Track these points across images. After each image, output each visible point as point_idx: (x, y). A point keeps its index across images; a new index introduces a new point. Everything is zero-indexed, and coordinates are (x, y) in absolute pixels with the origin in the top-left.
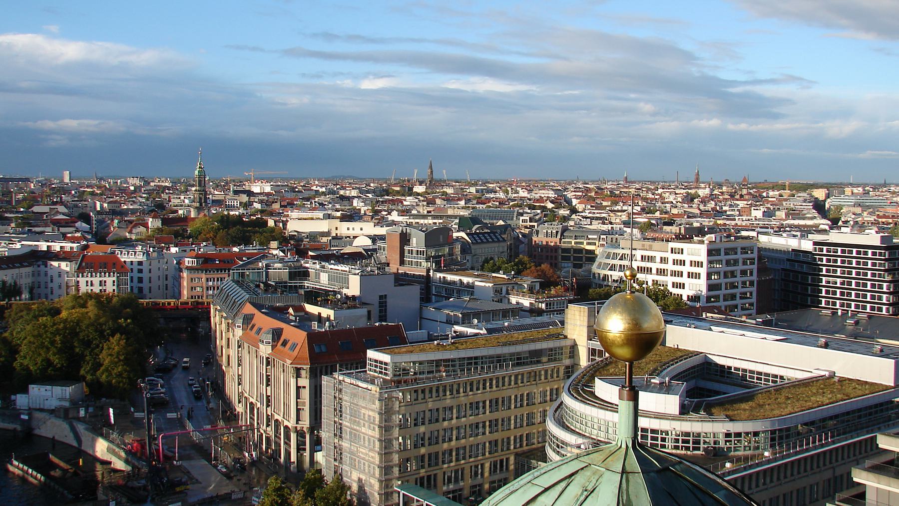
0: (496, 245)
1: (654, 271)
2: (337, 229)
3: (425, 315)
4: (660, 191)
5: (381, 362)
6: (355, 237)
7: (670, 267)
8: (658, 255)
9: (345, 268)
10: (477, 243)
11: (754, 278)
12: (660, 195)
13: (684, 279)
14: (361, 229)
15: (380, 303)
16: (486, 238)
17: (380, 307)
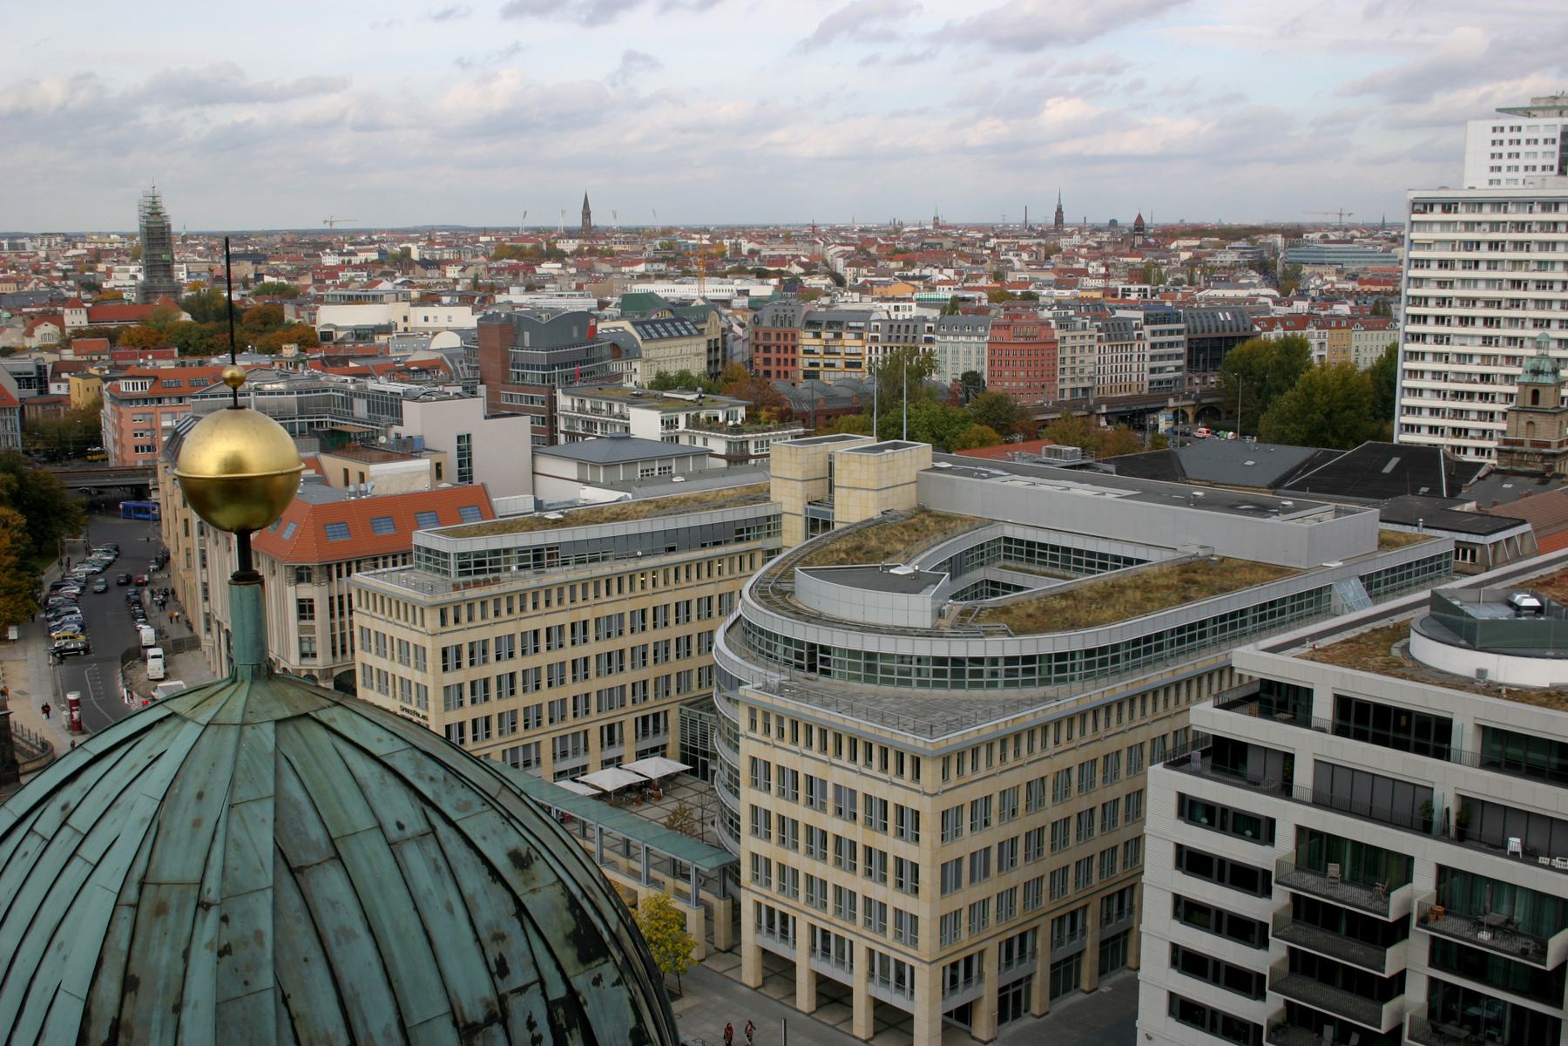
0: (687, 341)
2: (405, 319)
3: (539, 470)
4: (993, 242)
5: (437, 553)
6: (435, 334)
9: (398, 387)
10: (652, 338)
12: (993, 249)
16: (657, 331)
17: (459, 456)
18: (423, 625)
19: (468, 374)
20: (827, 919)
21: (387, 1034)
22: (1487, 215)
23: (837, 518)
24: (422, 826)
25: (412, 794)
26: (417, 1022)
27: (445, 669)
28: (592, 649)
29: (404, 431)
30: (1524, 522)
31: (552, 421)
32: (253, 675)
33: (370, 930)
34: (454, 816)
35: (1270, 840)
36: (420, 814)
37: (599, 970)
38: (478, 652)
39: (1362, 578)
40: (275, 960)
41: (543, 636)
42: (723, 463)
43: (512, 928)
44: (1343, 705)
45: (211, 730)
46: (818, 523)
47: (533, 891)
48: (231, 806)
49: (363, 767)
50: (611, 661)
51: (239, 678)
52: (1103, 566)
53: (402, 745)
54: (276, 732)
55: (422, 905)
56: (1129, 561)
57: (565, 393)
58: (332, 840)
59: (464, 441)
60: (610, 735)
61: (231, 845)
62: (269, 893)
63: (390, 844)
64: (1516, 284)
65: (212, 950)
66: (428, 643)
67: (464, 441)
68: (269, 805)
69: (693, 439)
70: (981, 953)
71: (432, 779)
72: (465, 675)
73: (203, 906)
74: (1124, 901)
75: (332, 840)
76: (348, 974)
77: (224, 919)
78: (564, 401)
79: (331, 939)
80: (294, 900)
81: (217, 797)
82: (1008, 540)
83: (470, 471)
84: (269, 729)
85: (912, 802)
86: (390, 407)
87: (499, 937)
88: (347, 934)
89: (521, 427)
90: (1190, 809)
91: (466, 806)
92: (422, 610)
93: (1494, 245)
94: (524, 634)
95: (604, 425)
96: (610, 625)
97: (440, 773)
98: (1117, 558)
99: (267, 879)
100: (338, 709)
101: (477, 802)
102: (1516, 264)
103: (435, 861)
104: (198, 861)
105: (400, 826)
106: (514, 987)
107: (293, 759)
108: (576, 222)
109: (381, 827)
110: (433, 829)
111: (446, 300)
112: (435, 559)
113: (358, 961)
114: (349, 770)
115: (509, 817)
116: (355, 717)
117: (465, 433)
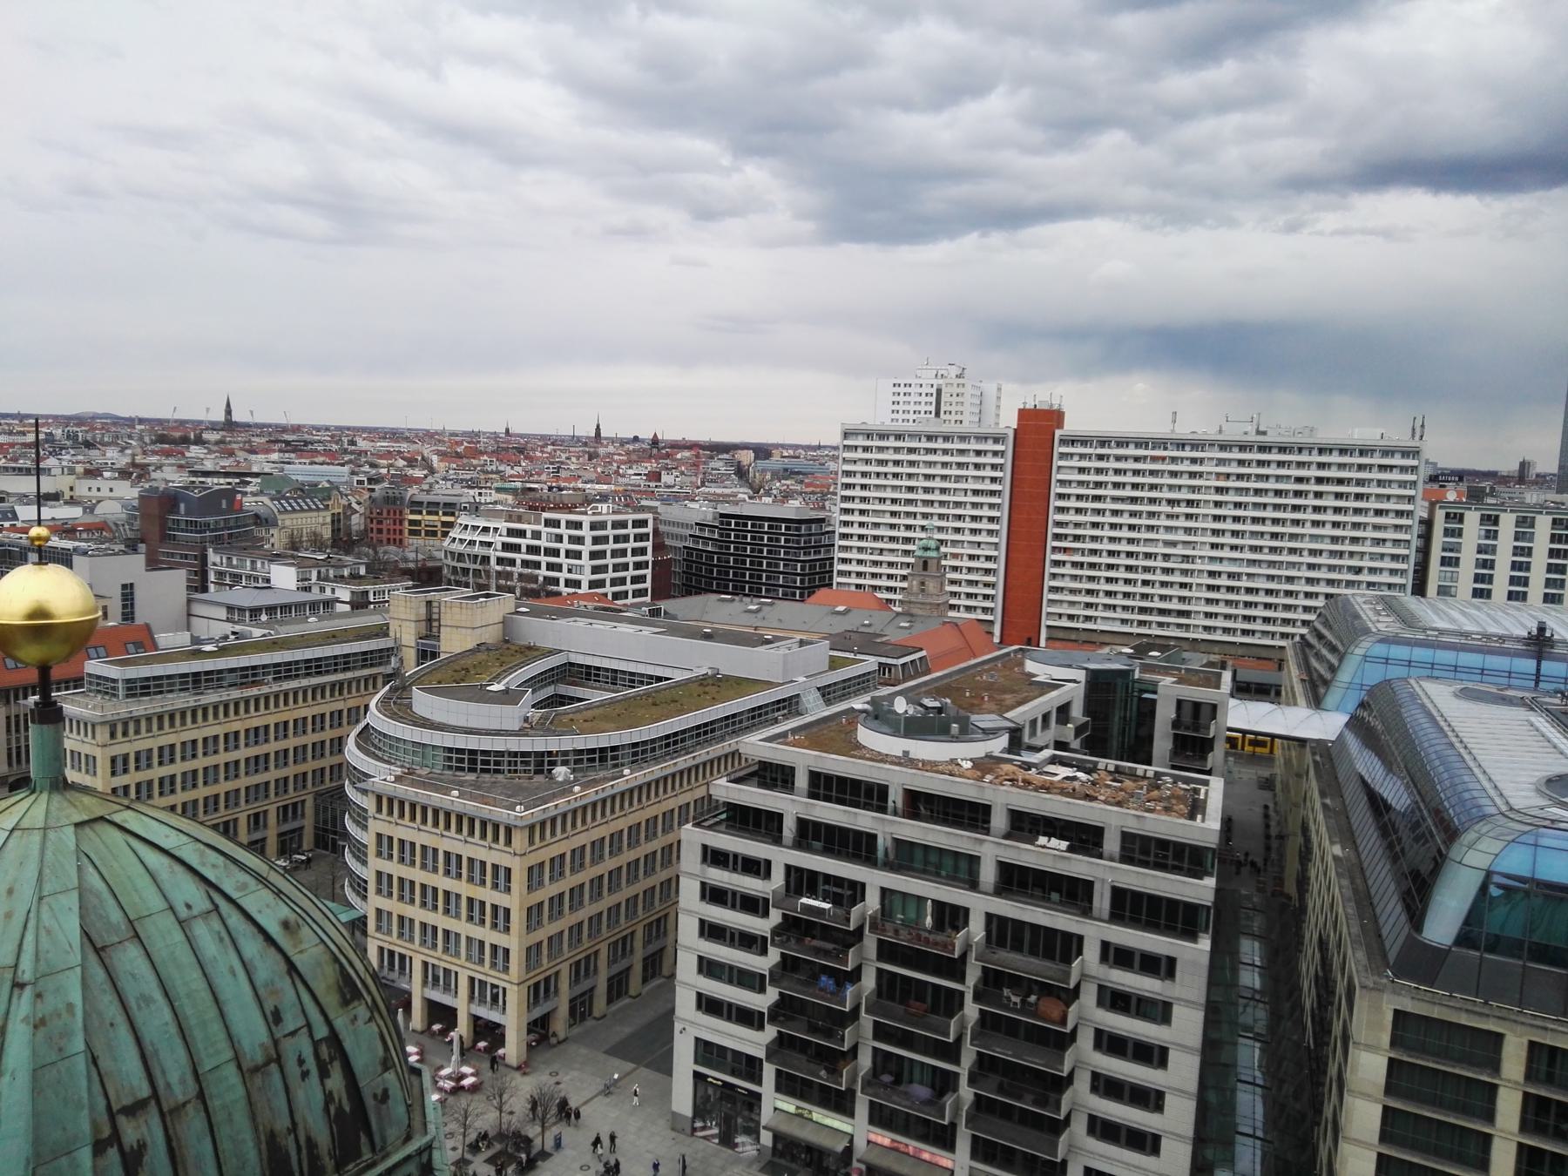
0: (315, 514)
1: (524, 549)
2: (71, 489)
5: (106, 679)
6: (99, 502)
7: (543, 543)
8: (528, 527)
11: (649, 557)
13: (562, 559)
14: (111, 490)
15: (123, 595)
17: (123, 600)
18: (94, 737)
19: (130, 535)
20: (439, 958)
21: (183, 1082)
22: (892, 443)
23: (442, 649)
24: (208, 905)
25: (197, 879)
26: (208, 1068)
27: (113, 774)
28: (242, 753)
30: (921, 649)
31: (204, 574)
32: (51, 786)
33: (166, 994)
34: (235, 895)
35: (768, 875)
36: (204, 896)
37: (354, 1012)
38: (143, 759)
39: (819, 689)
40: (85, 1026)
41: (200, 745)
42: (347, 608)
43: (285, 984)
44: (815, 777)
45: (17, 833)
46: (424, 655)
47: (301, 952)
48: (41, 898)
49: (152, 858)
50: (258, 763)
51: (38, 789)
52: (642, 683)
53: (185, 839)
54: (76, 834)
55: (209, 970)
56: (659, 679)
57: (216, 551)
58: (130, 922)
59: (128, 592)
60: (257, 820)
61: (43, 933)
62: (78, 970)
63: (180, 922)
64: (910, 489)
65: (28, 1024)
66: (98, 753)
67: (128, 592)
68: (75, 894)
69: (322, 590)
70: (557, 973)
71: (214, 866)
72: (131, 778)
73: (18, 985)
74: (662, 928)
75: (130, 922)
76: (150, 1033)
77: (39, 996)
78: (213, 557)
79: (132, 1003)
80: (99, 974)
81: (27, 892)
82: (572, 664)
83: (133, 613)
84: (72, 829)
85: (504, 860)
87: (275, 992)
88: (147, 1000)
89: (177, 580)
90: (715, 857)
91: (244, 887)
92: (93, 726)
93: (897, 463)
94: (183, 744)
95: (249, 577)
96: (257, 735)
97: (220, 860)
98: (651, 677)
99: (76, 958)
100: (130, 812)
101: (252, 882)
102: (910, 476)
103: (219, 933)
104: (11, 947)
105: (189, 907)
106: (286, 1032)
107: (92, 855)
108: (220, 416)
109: (171, 908)
110: (216, 908)
111: (106, 474)
112: (105, 687)
113: (156, 1021)
114: (142, 862)
115: (279, 893)
116: (143, 817)
117: (128, 582)
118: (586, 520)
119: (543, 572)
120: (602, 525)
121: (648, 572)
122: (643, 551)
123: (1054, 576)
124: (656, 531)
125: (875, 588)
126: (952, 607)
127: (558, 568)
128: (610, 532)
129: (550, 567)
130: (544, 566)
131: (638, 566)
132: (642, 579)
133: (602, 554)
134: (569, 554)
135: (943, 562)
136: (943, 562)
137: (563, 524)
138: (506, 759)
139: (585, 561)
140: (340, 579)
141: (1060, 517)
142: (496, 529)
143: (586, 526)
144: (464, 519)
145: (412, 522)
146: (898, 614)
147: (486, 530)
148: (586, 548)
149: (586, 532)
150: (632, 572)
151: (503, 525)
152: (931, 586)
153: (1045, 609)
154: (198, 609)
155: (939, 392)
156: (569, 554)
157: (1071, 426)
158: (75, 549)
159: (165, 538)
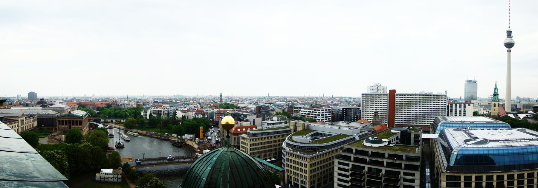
7: (314, 113)
11: (331, 115)
13: (317, 116)
20: (296, 177)
23: (297, 130)
27: (250, 146)
28: (268, 145)
29: (247, 119)
38: (254, 145)
46: (295, 131)
56: (332, 135)
59: (254, 120)
66: (249, 143)
67: (254, 120)
85: (306, 163)
86: (245, 116)
89: (260, 119)
95: (270, 119)
96: (270, 142)
118: (321, 109)
119: (314, 118)
120: (323, 110)
121: (331, 118)
122: (330, 114)
123: (396, 116)
124: (332, 111)
125: (368, 119)
126: (380, 122)
127: (316, 117)
128: (324, 111)
129: (315, 117)
130: (314, 117)
131: (329, 117)
132: (330, 119)
133: (323, 115)
134: (318, 115)
135: (379, 115)
136: (379, 115)
137: (317, 110)
138: (306, 147)
139: (321, 116)
140: (283, 119)
141: (396, 107)
142: (307, 111)
143: (321, 110)
144: (302, 110)
145: (294, 110)
146: (371, 123)
147: (305, 111)
148: (321, 114)
149: (321, 111)
150: (328, 118)
151: (308, 111)
152: (377, 119)
153: (395, 122)
154: (263, 123)
155: (377, 88)
156: (318, 115)
157: (398, 93)
158: (247, 114)
159: (259, 113)
